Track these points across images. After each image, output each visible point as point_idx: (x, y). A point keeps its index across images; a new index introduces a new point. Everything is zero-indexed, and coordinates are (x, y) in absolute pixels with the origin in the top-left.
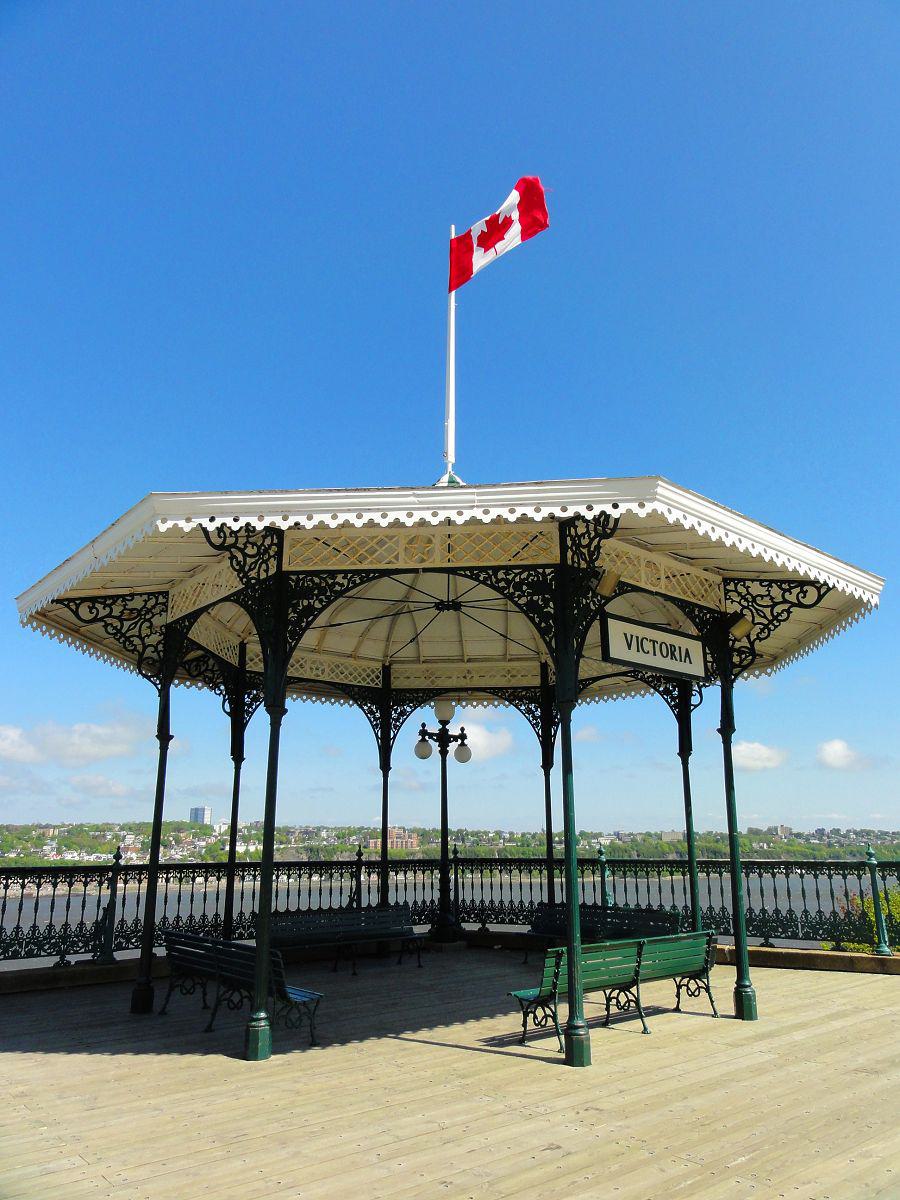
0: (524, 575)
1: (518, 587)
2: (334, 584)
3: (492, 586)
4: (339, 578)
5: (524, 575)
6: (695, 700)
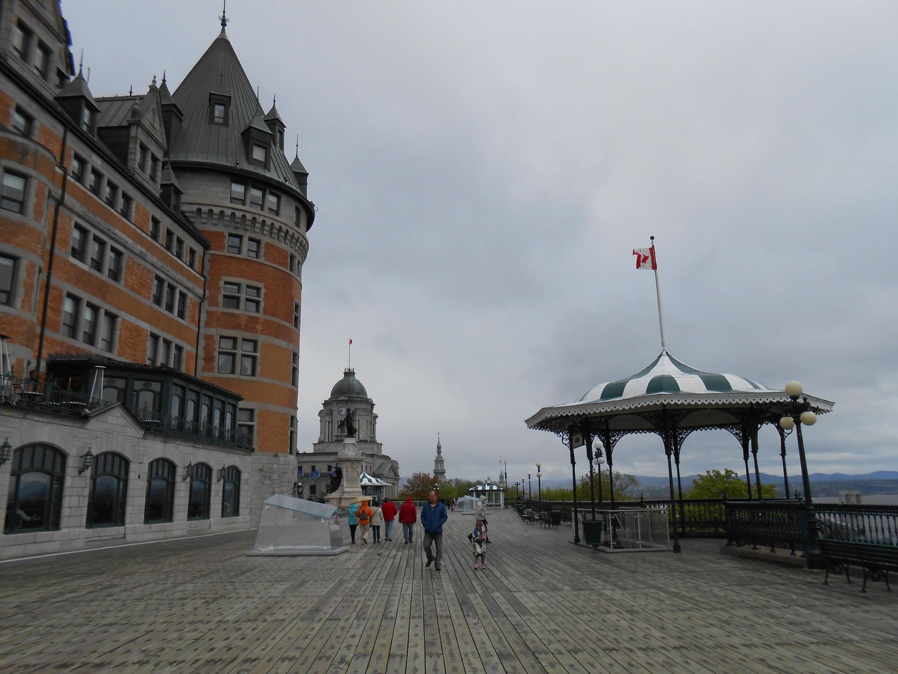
4: (684, 411)
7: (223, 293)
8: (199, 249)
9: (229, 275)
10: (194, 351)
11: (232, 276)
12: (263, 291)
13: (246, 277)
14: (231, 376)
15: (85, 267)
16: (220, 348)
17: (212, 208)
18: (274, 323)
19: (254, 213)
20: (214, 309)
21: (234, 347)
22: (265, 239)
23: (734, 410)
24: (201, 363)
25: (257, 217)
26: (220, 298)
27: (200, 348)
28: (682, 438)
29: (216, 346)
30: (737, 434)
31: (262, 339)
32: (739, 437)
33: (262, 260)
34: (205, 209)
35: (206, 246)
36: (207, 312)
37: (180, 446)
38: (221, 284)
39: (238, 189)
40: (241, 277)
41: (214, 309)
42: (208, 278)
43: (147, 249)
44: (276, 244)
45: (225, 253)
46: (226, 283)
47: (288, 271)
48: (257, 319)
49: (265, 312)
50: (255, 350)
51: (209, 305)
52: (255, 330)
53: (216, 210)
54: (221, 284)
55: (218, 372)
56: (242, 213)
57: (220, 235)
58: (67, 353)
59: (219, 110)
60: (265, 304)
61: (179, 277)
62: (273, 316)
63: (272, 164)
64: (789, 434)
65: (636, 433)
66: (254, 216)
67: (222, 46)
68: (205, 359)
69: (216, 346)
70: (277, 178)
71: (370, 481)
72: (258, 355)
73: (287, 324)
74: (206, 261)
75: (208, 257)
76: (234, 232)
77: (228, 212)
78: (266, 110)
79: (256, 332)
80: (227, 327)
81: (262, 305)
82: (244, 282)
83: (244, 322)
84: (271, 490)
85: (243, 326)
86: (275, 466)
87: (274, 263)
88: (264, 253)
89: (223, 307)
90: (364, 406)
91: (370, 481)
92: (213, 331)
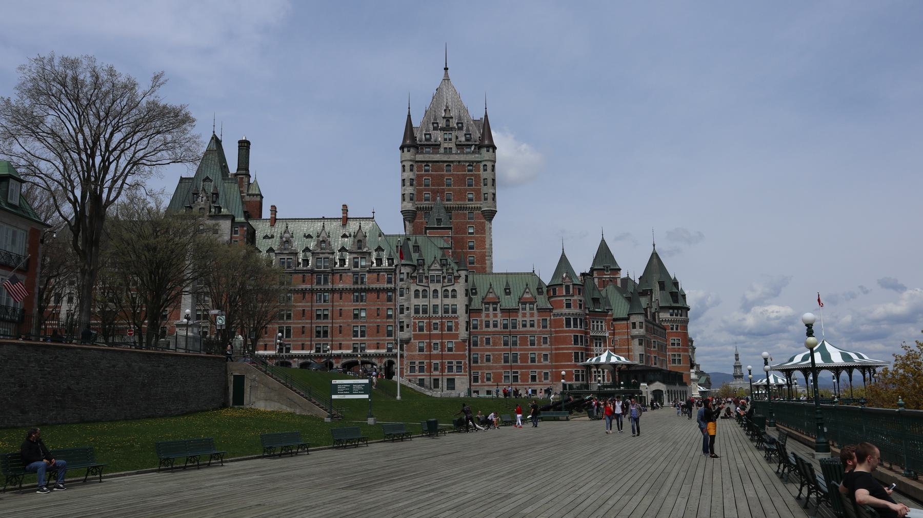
26: (671, 344)
31: (682, 354)
33: (679, 331)
39: (671, 311)
45: (670, 331)
53: (667, 319)
67: (655, 256)
71: (700, 388)
78: (673, 278)
83: (677, 350)
92: (670, 353)
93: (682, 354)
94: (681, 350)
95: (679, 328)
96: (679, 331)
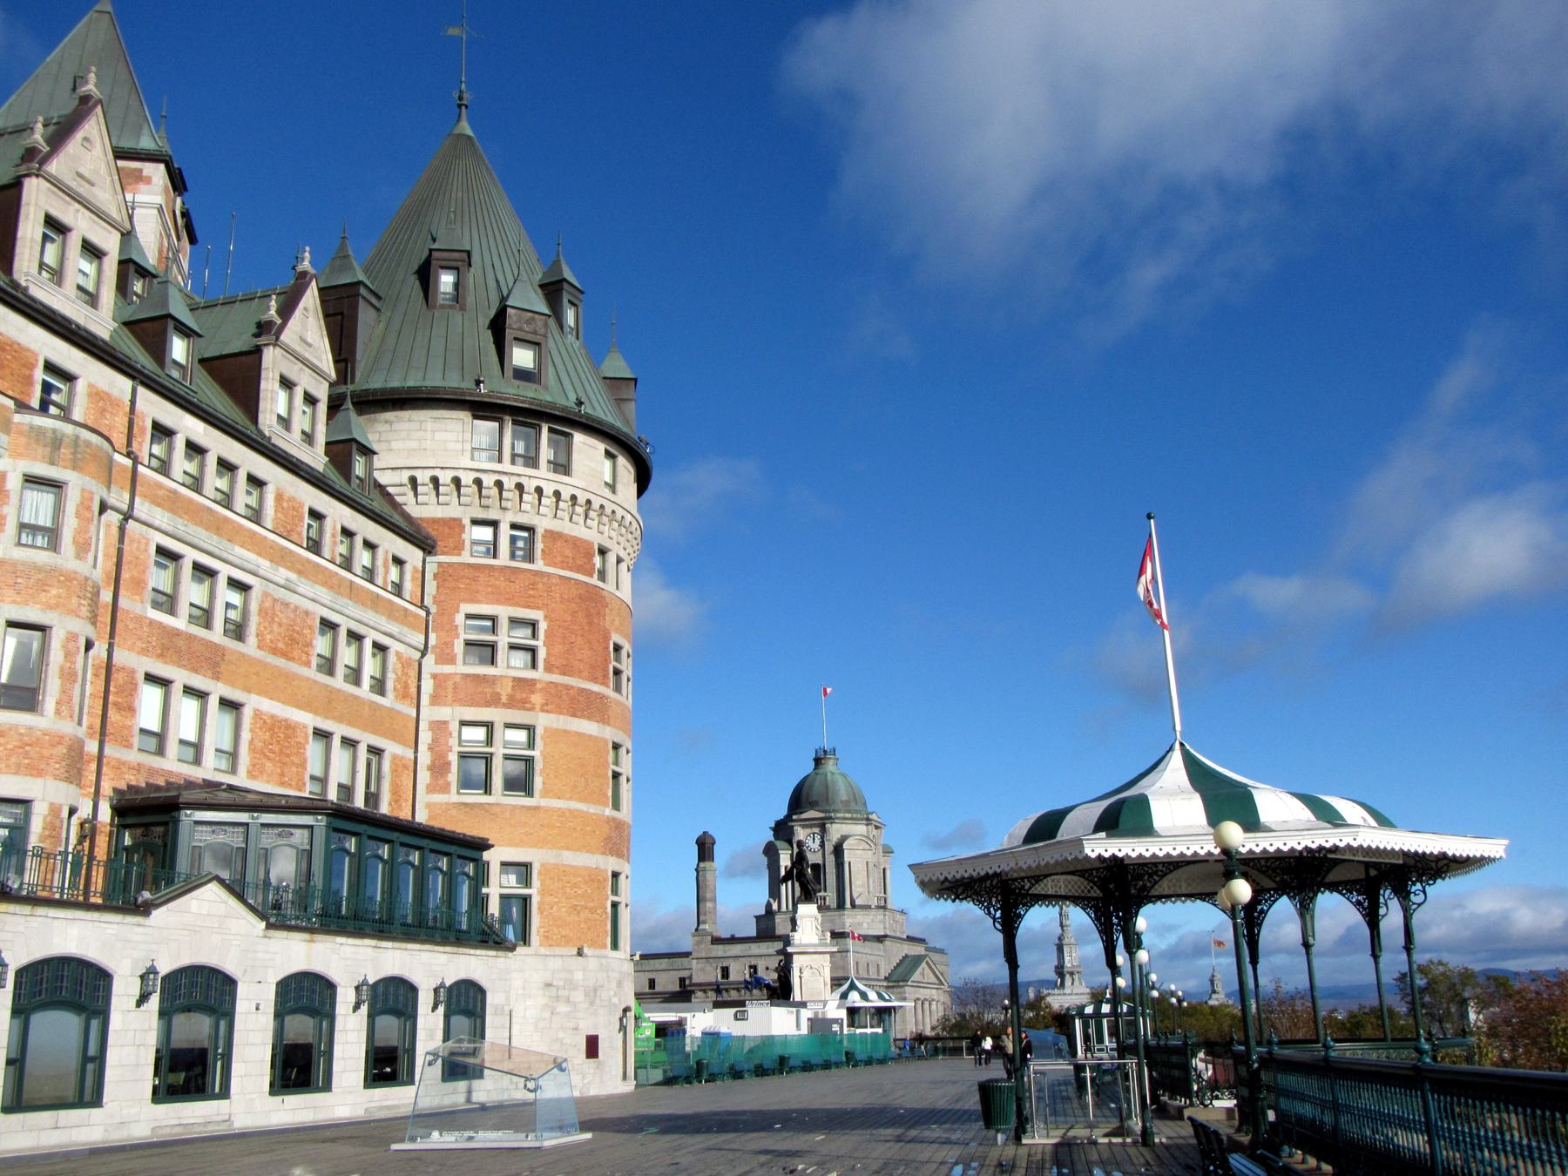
0: (1277, 863)
1: (1274, 870)
2: (1157, 871)
3: (1257, 870)
4: (1160, 867)
5: (1277, 863)
6: (1382, 911)
7: (463, 636)
8: (413, 555)
9: (473, 600)
10: (410, 754)
11: (479, 602)
12: (543, 627)
13: (509, 601)
14: (485, 799)
15: (180, 623)
16: (460, 745)
17: (437, 473)
18: (568, 687)
19: (519, 475)
20: (447, 669)
21: (489, 741)
22: (543, 524)
23: (1263, 862)
24: (424, 777)
25: (524, 481)
26: (459, 647)
27: (423, 747)
28: (1262, 910)
29: (453, 742)
30: (1358, 903)
31: (543, 721)
32: (1363, 908)
33: (539, 565)
34: (423, 477)
35: (426, 545)
36: (434, 676)
37: (343, 947)
38: (460, 619)
40: (498, 602)
41: (447, 669)
42: (433, 609)
43: (299, 573)
44: (566, 532)
45: (465, 557)
46: (469, 617)
47: (594, 581)
48: (531, 683)
49: (549, 668)
50: (531, 744)
51: (436, 663)
52: (528, 706)
54: (460, 619)
55: (458, 793)
56: (496, 477)
57: (455, 524)
58: (147, 784)
59: (446, 280)
60: (548, 650)
61: (370, 616)
62: (564, 674)
63: (551, 370)
64: (1419, 905)
65: (1184, 902)
66: (518, 480)
68: (431, 768)
69: (453, 742)
70: (562, 401)
71: (864, 996)
72: (536, 753)
73: (596, 688)
74: (429, 576)
75: (431, 569)
76: (482, 515)
77: (467, 479)
79: (532, 709)
80: (473, 703)
81: (542, 654)
82: (504, 612)
83: (505, 690)
84: (571, 1025)
85: (504, 699)
86: (579, 976)
87: (563, 569)
88: (543, 551)
89: (464, 663)
90: (861, 829)
91: (864, 996)
92: (450, 713)
93: (543, 721)
94: (537, 699)
95: (539, 546)
96: (539, 565)
